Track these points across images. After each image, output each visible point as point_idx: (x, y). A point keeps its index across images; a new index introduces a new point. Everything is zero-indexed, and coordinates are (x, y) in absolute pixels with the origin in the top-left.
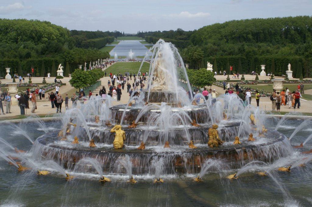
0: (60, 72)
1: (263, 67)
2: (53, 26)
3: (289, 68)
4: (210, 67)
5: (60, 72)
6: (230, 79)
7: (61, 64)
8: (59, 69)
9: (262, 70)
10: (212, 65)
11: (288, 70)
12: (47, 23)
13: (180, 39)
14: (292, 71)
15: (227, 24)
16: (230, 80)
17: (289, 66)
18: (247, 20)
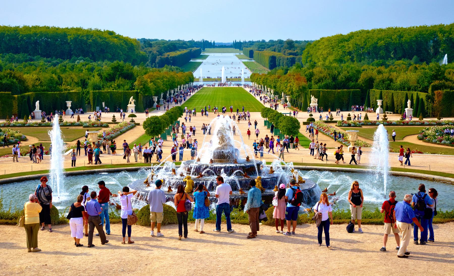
0: (131, 106)
1: (379, 103)
2: (118, 37)
3: (409, 105)
4: (314, 102)
5: (131, 106)
6: (333, 119)
7: (132, 97)
8: (131, 103)
9: (377, 107)
10: (317, 100)
11: (407, 107)
12: (111, 33)
13: (290, 54)
14: (412, 109)
15: (351, 36)
16: (333, 120)
17: (409, 102)
18: (381, 30)
